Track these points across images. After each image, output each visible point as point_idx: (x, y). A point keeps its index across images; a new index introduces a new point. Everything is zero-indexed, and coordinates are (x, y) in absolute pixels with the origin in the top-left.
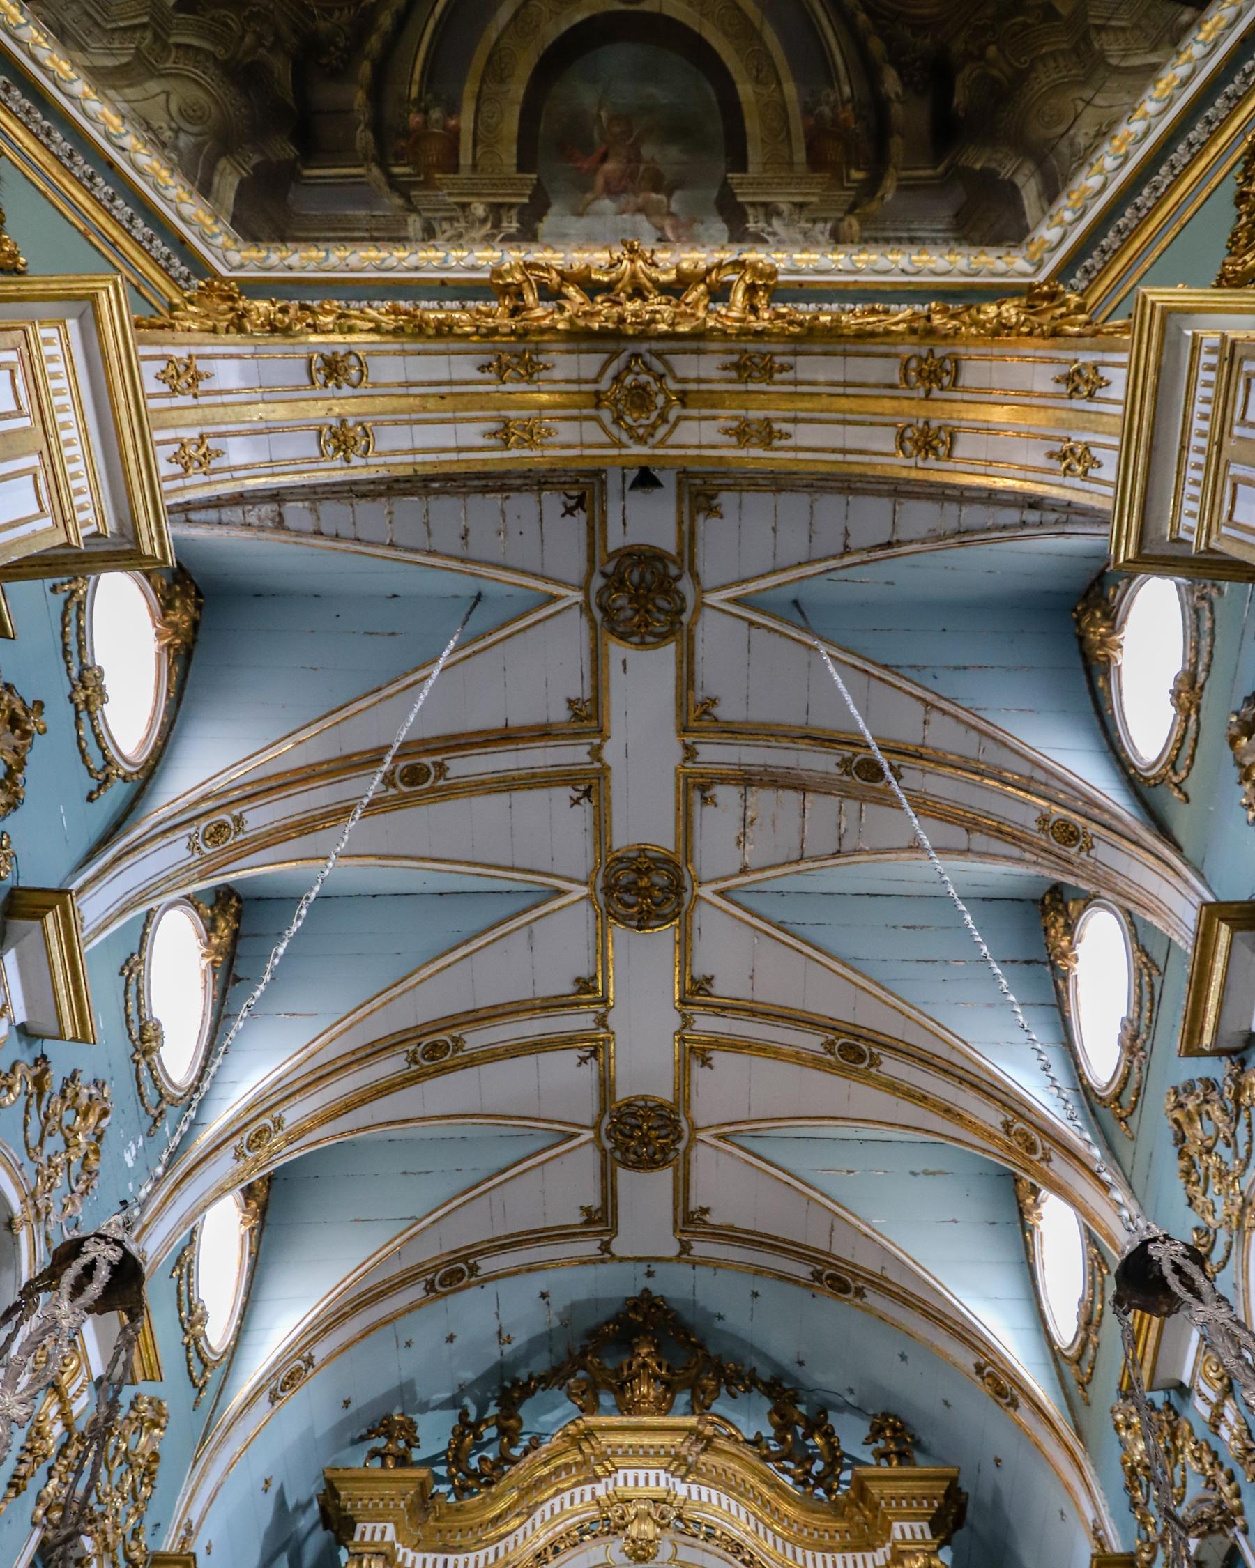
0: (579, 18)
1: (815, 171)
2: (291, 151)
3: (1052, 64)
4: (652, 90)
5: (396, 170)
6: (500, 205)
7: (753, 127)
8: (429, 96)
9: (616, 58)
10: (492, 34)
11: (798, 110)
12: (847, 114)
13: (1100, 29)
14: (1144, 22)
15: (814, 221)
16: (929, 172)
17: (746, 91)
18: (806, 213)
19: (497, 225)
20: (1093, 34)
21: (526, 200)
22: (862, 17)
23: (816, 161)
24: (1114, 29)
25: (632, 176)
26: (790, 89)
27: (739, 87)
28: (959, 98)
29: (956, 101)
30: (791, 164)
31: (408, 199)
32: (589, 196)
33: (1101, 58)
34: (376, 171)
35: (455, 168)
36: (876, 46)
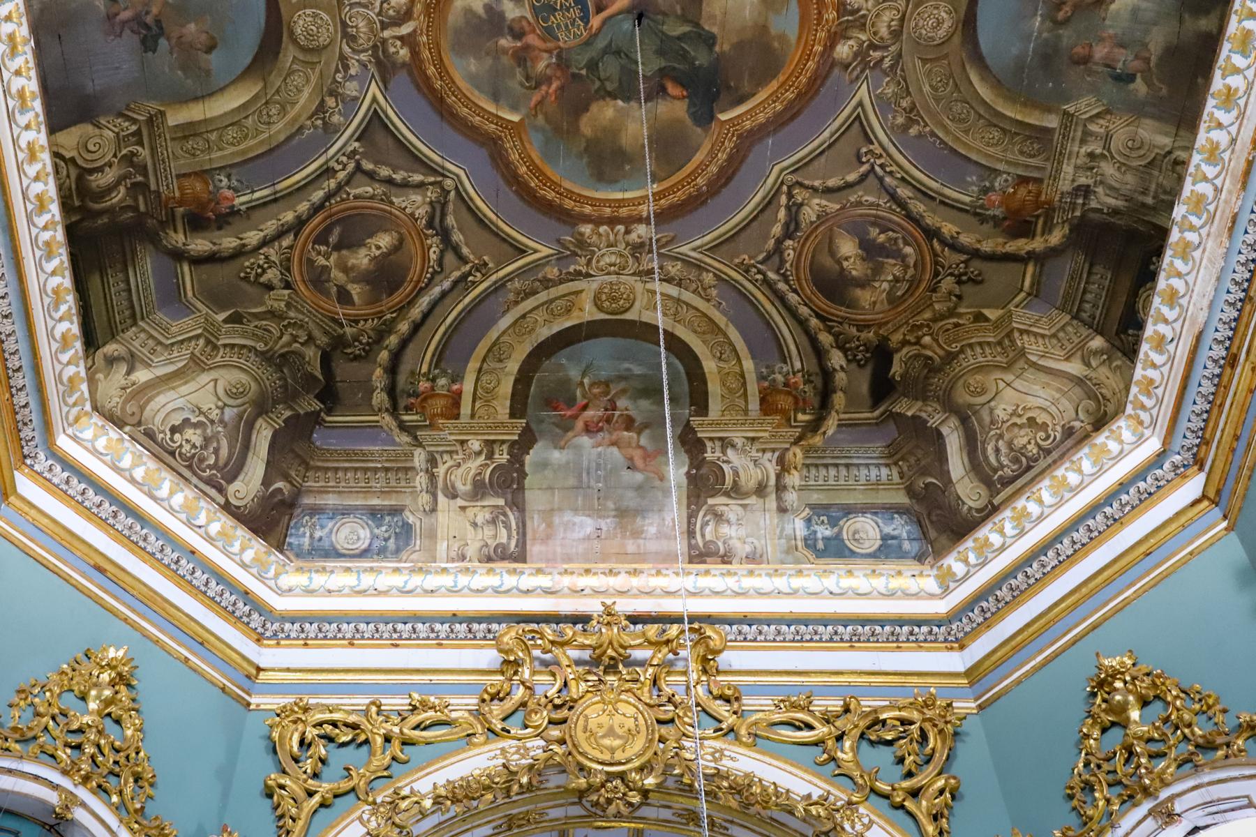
0: (568, 324)
1: (765, 415)
2: (317, 405)
3: (978, 350)
4: (626, 365)
5: (406, 418)
6: (494, 441)
7: (714, 387)
8: (437, 371)
9: (598, 349)
10: (493, 334)
11: (754, 376)
12: (799, 378)
13: (1022, 332)
14: (1061, 335)
15: (764, 451)
16: (869, 415)
17: (709, 365)
18: (757, 445)
19: (490, 456)
20: (1016, 334)
21: (516, 438)
22: (814, 322)
23: (767, 406)
24: (1036, 335)
25: (608, 420)
26: (748, 365)
27: (704, 363)
28: (897, 369)
29: (893, 371)
30: (746, 412)
31: (416, 438)
32: (570, 434)
33: (1022, 353)
34: (387, 419)
35: (457, 417)
36: (825, 339)
